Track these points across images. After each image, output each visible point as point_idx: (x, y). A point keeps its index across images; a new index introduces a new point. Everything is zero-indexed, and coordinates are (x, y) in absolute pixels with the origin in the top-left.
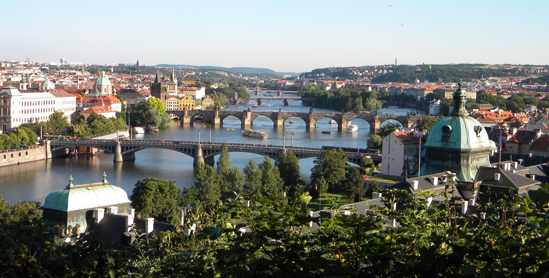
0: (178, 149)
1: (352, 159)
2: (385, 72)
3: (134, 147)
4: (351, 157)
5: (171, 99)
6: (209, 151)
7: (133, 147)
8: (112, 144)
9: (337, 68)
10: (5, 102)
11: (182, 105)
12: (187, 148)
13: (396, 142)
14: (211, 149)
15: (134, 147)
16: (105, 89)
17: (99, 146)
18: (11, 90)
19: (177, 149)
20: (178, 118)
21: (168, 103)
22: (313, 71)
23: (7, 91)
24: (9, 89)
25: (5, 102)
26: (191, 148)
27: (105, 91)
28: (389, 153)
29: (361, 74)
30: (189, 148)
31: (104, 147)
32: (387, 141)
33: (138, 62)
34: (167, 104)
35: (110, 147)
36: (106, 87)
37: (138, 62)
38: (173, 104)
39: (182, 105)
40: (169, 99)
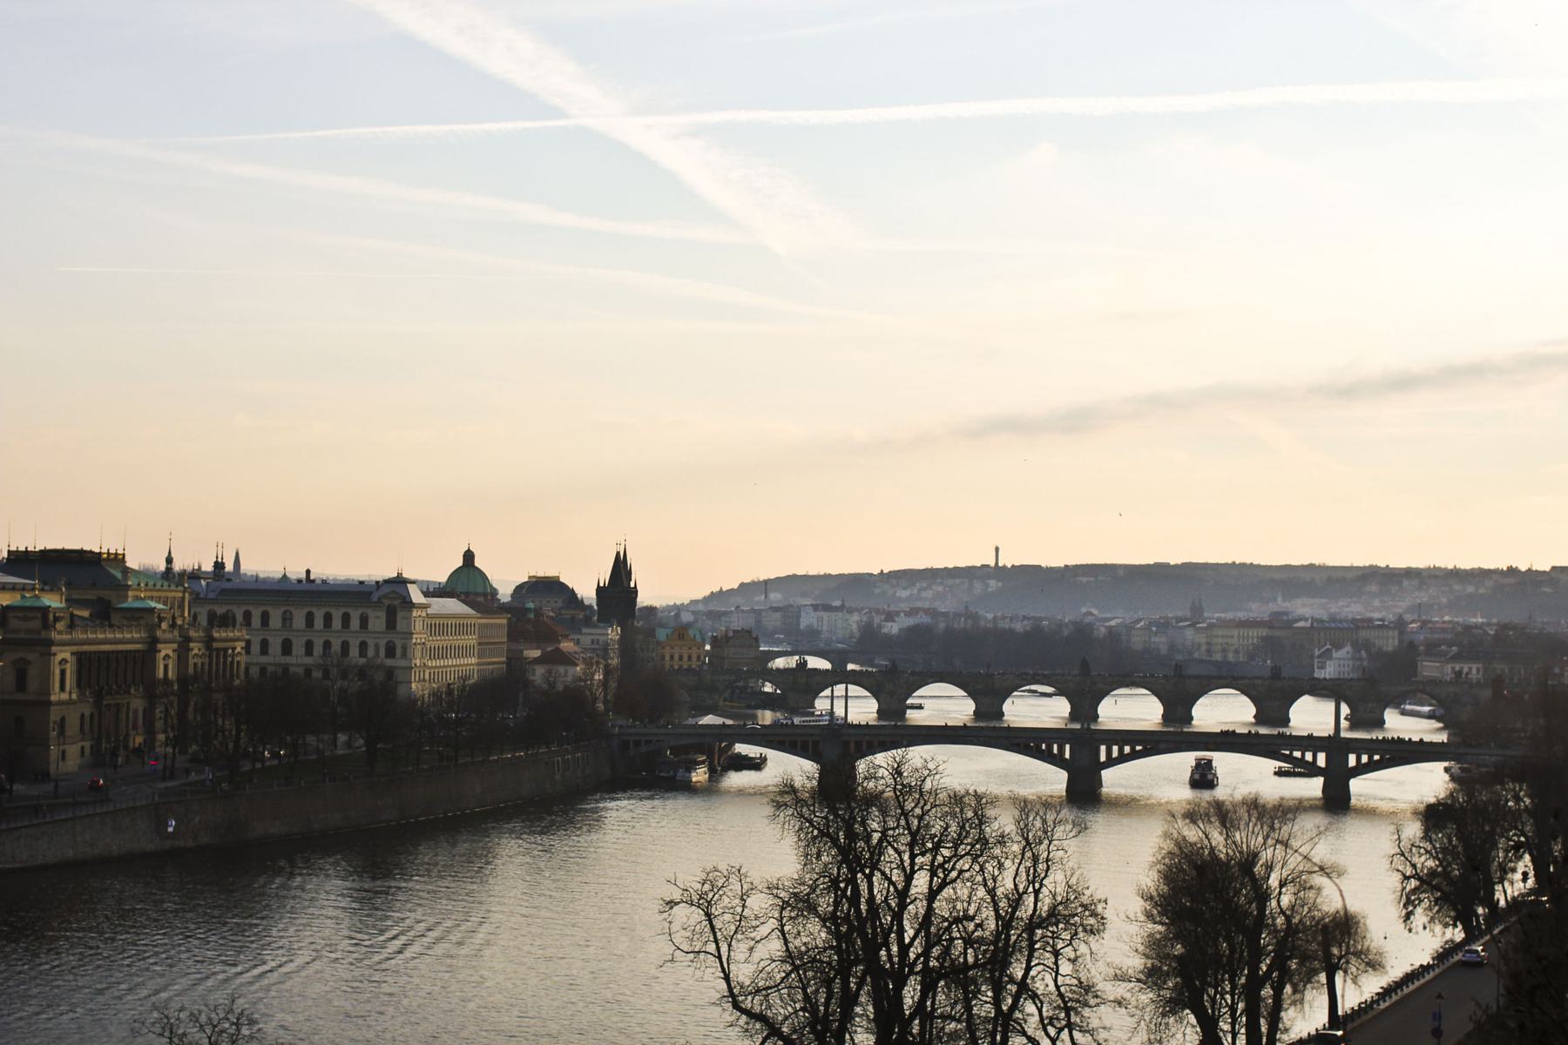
0: (1018, 745)
8: (811, 735)
10: (391, 624)
17: (773, 741)
18: (408, 585)
22: (742, 585)
23: (398, 589)
25: (391, 624)
37: (237, 554)
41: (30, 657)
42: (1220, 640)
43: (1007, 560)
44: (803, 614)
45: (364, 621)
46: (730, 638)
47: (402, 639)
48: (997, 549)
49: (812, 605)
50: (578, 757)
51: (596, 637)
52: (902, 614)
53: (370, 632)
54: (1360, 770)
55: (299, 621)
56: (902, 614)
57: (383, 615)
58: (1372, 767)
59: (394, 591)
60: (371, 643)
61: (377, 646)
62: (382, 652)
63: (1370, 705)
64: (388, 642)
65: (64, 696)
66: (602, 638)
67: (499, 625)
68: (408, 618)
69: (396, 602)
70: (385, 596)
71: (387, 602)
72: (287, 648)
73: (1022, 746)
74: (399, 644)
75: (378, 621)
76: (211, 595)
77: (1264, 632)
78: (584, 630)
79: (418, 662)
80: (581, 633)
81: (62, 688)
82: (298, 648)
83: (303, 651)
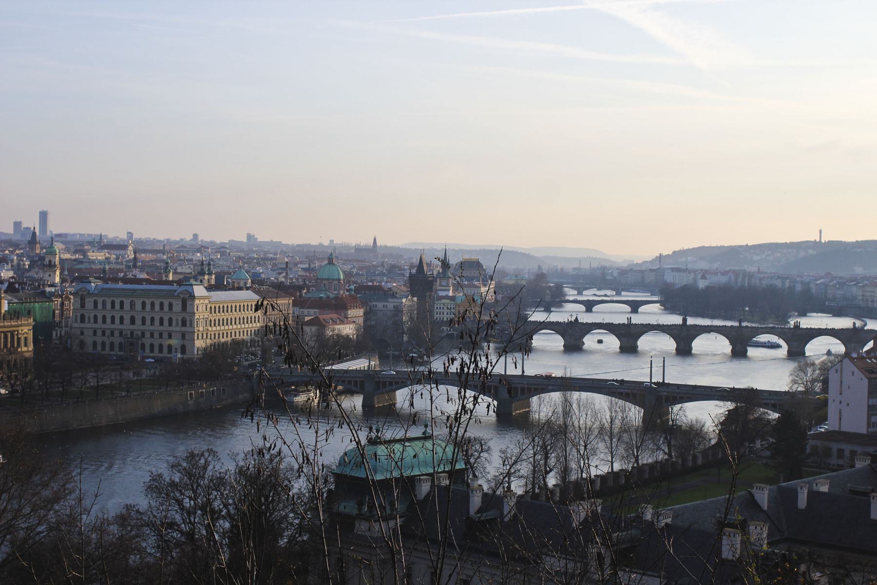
1: (770, 405)
2: (802, 254)
3: (397, 383)
4: (768, 401)
5: (444, 301)
6: (523, 389)
7: (394, 383)
8: (359, 377)
9: (717, 247)
10: (184, 307)
13: (853, 375)
14: (526, 386)
20: (455, 335)
21: (437, 308)
22: (674, 252)
24: (192, 285)
25: (184, 307)
28: (841, 394)
31: (346, 382)
32: (837, 372)
33: (375, 240)
34: (436, 310)
35: (356, 382)
37: (375, 240)
38: (446, 311)
40: (439, 302)
42: (869, 294)
44: (666, 274)
45: (171, 306)
46: (499, 301)
47: (190, 316)
48: (821, 231)
49: (671, 268)
50: (213, 391)
51: (395, 304)
52: (719, 274)
53: (174, 312)
56: (719, 274)
57: (180, 303)
59: (186, 290)
61: (177, 320)
63: (853, 345)
64: (183, 318)
68: (193, 305)
70: (181, 293)
71: (182, 296)
72: (133, 320)
73: (472, 386)
74: (188, 319)
75: (177, 307)
76: (96, 292)
78: (390, 300)
79: (201, 329)
80: (388, 302)
82: (138, 321)
83: (140, 322)
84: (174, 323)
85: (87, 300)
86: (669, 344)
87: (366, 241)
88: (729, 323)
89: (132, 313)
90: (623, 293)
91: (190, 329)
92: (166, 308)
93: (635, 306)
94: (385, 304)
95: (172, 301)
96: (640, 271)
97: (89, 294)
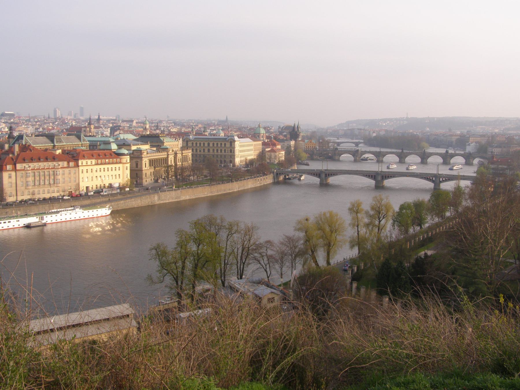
0: (364, 175)
10: (231, 145)
11: (312, 147)
12: (370, 175)
15: (334, 174)
16: (262, 136)
19: (364, 175)
23: (232, 137)
24: (234, 136)
26: (373, 175)
27: (262, 138)
29: (384, 124)
30: (372, 174)
33: (227, 118)
36: (262, 135)
39: (312, 147)
41: (138, 160)
43: (409, 117)
45: (225, 144)
54: (443, 181)
55: (211, 145)
57: (229, 143)
58: (446, 181)
60: (227, 149)
61: (228, 150)
62: (229, 152)
65: (146, 168)
66: (289, 144)
67: (260, 144)
68: (234, 144)
69: (232, 141)
70: (229, 139)
74: (233, 150)
75: (228, 145)
76: (193, 139)
77: (459, 137)
78: (285, 142)
79: (237, 154)
81: (146, 167)
84: (227, 151)
85: (189, 143)
86: (440, 160)
87: (223, 118)
88: (398, 151)
89: (209, 148)
90: (340, 139)
91: (233, 154)
92: (223, 145)
93: (357, 144)
94: (284, 143)
95: (226, 142)
96: (343, 130)
97: (190, 140)
